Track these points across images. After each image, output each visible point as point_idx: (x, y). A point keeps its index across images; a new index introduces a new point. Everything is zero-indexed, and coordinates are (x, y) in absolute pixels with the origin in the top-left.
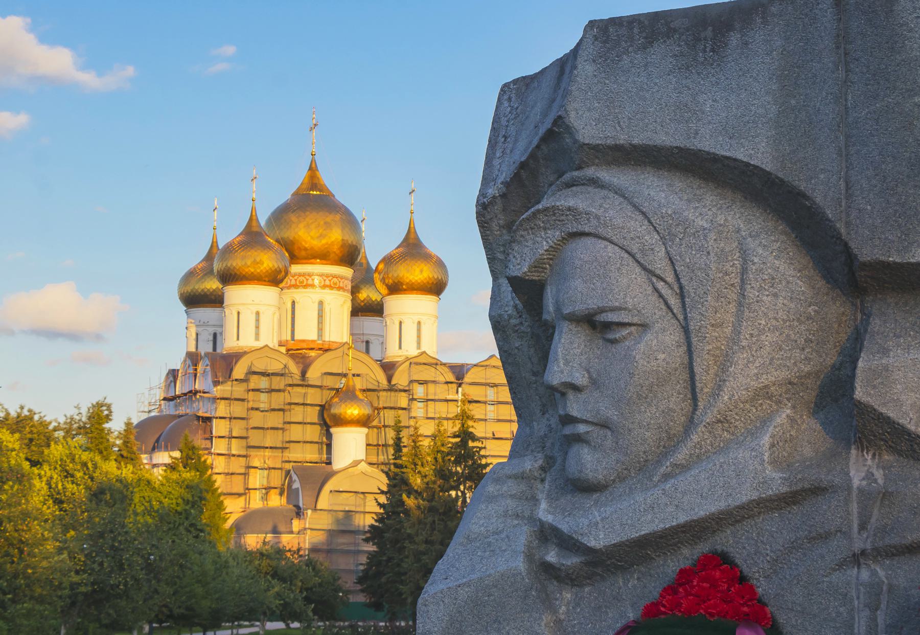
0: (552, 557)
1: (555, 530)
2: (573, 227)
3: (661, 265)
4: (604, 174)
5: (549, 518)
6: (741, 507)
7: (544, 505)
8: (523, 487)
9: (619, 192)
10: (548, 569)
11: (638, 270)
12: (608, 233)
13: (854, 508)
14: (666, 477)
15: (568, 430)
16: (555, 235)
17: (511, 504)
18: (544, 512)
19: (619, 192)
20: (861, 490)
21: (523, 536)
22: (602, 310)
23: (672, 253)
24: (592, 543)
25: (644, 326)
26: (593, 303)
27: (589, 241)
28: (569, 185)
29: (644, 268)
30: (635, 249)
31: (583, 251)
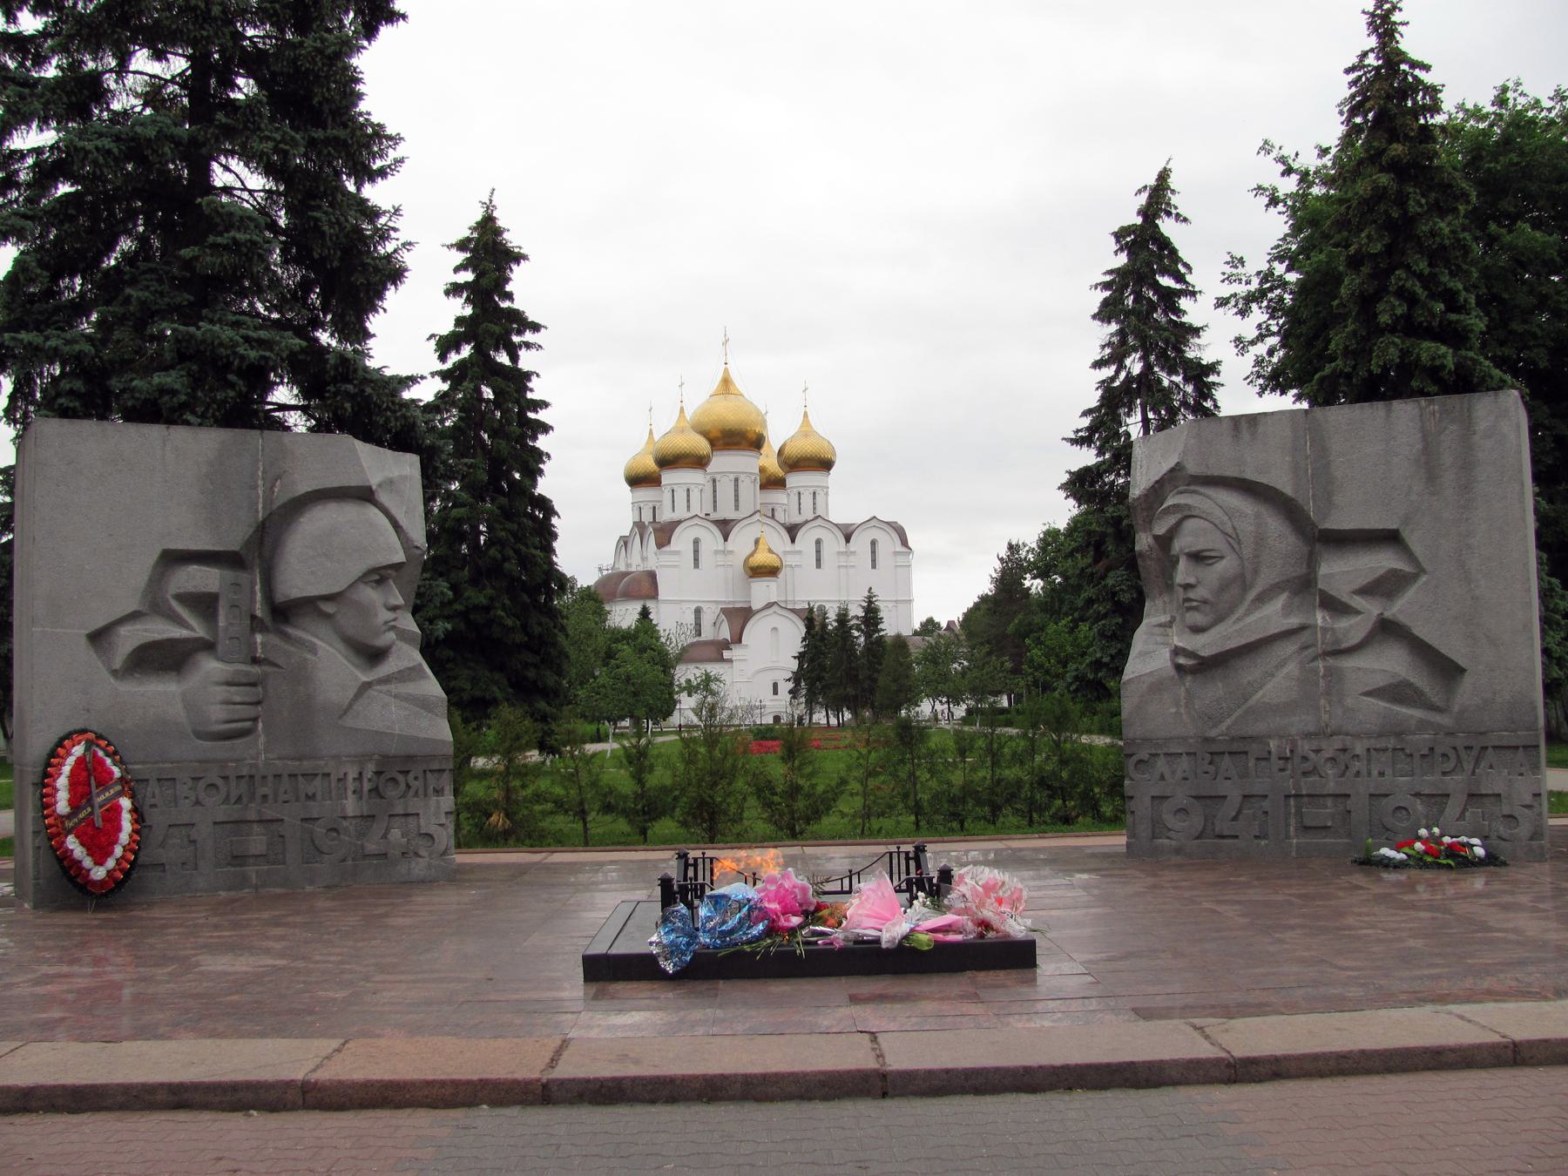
0: (1182, 661)
1: (1184, 650)
2: (1187, 513)
3: (1230, 531)
4: (1202, 490)
5: (1181, 644)
6: (1271, 636)
7: (1175, 638)
8: (1162, 629)
9: (1208, 497)
10: (1179, 668)
11: (1219, 532)
12: (1204, 515)
13: (1319, 635)
14: (1234, 623)
15: (1187, 604)
16: (1179, 516)
17: (1159, 639)
18: (1177, 641)
19: (1208, 497)
20: (1322, 628)
21: (1166, 653)
22: (1203, 551)
23: (1235, 524)
24: (1202, 654)
25: (1222, 558)
26: (1199, 548)
27: (1196, 520)
28: (1181, 493)
29: (1222, 532)
30: (1217, 522)
31: (1190, 525)
